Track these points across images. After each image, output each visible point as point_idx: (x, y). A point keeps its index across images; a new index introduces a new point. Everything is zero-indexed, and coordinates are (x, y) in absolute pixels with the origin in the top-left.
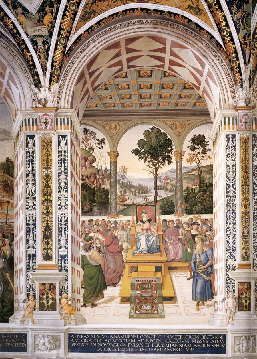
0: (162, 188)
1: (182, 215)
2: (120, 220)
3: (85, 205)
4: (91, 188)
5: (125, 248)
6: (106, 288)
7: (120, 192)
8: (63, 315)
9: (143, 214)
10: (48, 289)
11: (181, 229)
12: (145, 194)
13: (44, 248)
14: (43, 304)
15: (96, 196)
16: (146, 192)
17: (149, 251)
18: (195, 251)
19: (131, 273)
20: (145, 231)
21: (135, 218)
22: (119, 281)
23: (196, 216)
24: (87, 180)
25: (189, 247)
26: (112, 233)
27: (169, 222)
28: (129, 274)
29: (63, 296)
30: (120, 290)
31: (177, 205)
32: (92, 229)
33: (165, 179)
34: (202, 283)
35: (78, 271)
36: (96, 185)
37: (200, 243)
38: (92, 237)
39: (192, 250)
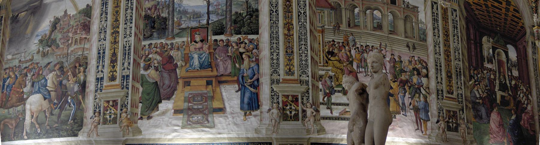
0: (213, 13)
1: (232, 35)
2: (176, 42)
3: (146, 32)
4: (152, 17)
5: (180, 66)
6: (161, 101)
7: (177, 18)
8: (122, 128)
9: (196, 36)
10: (111, 106)
11: (230, 48)
12: (198, 18)
13: (110, 72)
14: (107, 119)
15: (156, 24)
16: (200, 17)
17: (201, 67)
18: (242, 67)
19: (184, 87)
20: (197, 50)
21: (189, 39)
22: (173, 95)
23: (244, 36)
24: (149, 11)
25: (237, 63)
26: (168, 54)
27: (220, 41)
28: (183, 89)
29: (123, 111)
30: (174, 103)
31: (226, 27)
32: (151, 51)
33: (216, 5)
34: (249, 95)
35: (137, 88)
36: (156, 15)
37: (247, 59)
38: (151, 59)
39: (240, 66)
